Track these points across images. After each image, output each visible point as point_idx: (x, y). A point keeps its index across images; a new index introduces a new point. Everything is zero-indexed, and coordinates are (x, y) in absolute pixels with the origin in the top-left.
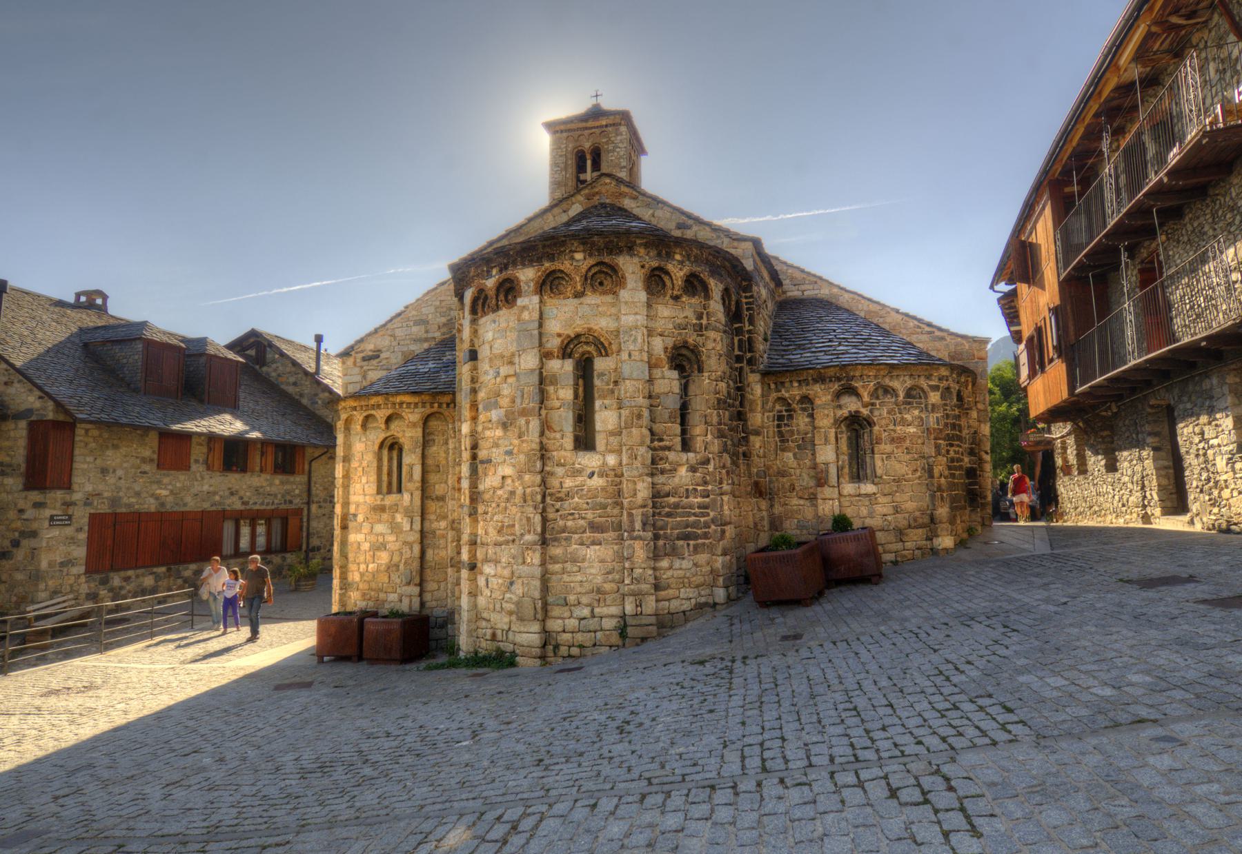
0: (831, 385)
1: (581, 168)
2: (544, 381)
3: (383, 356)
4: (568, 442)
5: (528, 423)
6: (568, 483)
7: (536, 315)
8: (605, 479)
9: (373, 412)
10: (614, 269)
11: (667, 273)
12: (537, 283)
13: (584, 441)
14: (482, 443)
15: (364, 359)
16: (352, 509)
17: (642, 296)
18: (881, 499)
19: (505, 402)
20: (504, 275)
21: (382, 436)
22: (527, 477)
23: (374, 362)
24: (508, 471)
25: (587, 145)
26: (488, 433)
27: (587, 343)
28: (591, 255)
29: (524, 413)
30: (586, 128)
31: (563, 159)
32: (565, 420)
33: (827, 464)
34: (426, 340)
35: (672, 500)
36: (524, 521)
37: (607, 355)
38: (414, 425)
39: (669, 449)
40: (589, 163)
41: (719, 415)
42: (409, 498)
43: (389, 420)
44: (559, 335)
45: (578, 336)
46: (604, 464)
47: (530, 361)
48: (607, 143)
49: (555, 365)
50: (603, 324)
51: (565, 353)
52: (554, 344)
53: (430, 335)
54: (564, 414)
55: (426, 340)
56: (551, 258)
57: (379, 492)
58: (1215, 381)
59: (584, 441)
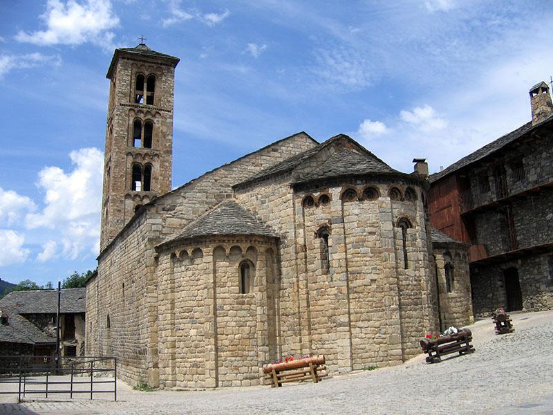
9: (239, 244)
10: (413, 191)
15: (163, 209)
16: (219, 302)
18: (458, 300)
20: (369, 185)
21: (241, 259)
24: (375, 277)
25: (147, 73)
29: (386, 250)
30: (147, 62)
37: (411, 227)
38: (262, 254)
40: (145, 85)
44: (397, 217)
46: (415, 275)
50: (409, 214)
52: (396, 220)
53: (208, 200)
56: (393, 182)
58: (542, 259)
59: (406, 267)
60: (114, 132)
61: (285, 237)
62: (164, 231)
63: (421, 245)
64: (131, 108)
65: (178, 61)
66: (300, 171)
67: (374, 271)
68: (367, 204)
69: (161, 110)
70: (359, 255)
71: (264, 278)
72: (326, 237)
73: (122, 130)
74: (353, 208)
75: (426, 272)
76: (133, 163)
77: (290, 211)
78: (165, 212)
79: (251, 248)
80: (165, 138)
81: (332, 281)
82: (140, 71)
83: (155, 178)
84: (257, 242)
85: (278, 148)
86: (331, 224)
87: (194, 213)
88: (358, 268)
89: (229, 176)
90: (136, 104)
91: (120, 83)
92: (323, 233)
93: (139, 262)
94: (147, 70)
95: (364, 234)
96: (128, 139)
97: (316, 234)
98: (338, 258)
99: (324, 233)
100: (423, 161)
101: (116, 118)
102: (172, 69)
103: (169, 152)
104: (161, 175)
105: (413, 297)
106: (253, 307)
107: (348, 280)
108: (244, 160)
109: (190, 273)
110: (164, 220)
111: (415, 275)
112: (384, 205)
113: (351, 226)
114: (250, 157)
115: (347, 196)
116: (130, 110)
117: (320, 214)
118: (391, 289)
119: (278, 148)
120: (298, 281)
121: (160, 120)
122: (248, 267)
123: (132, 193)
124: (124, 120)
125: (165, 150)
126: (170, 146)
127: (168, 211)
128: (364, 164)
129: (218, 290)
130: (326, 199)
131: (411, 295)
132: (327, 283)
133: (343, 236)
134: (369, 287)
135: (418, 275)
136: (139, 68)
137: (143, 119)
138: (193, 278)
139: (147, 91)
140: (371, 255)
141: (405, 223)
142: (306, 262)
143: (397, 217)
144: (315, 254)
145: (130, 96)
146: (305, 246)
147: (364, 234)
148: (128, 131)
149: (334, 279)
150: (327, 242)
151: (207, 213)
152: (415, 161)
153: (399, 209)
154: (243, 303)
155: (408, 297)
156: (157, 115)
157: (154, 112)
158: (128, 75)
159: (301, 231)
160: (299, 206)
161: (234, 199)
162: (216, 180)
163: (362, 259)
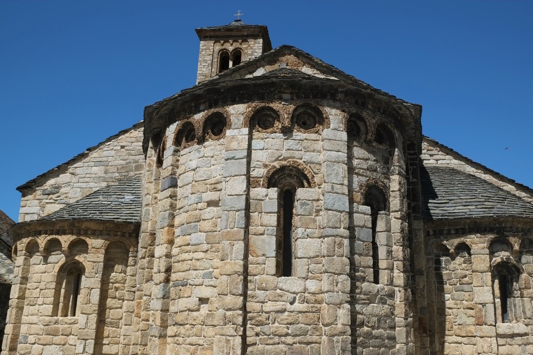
4: (271, 265)
6: (269, 306)
7: (245, 145)
8: (305, 304)
11: (362, 120)
13: (285, 267)
14: (176, 266)
17: (344, 136)
22: (229, 300)
23: (54, 197)
24: (205, 292)
25: (231, 48)
26: (185, 256)
27: (290, 176)
28: (298, 97)
29: (228, 236)
31: (210, 57)
32: (267, 245)
35: (366, 329)
36: (223, 343)
37: (310, 186)
39: (363, 279)
41: (403, 251)
42: (84, 320)
43: (73, 245)
44: (266, 166)
45: (283, 168)
46: (305, 290)
47: (239, 185)
49: (258, 192)
51: (271, 182)
57: (55, 313)
59: (285, 267)
67: (207, 281)
78: (46, 197)
82: (223, 47)
91: (201, 64)
95: (200, 205)
105: (289, 340)
106: (72, 339)
111: (305, 290)
112: (234, 145)
118: (226, 321)
127: (49, 194)
131: (287, 335)
134: (195, 314)
140: (205, 247)
143: (266, 166)
147: (200, 205)
154: (55, 334)
155: (276, 339)
158: (209, 55)
162: (123, 147)
163: (191, 255)
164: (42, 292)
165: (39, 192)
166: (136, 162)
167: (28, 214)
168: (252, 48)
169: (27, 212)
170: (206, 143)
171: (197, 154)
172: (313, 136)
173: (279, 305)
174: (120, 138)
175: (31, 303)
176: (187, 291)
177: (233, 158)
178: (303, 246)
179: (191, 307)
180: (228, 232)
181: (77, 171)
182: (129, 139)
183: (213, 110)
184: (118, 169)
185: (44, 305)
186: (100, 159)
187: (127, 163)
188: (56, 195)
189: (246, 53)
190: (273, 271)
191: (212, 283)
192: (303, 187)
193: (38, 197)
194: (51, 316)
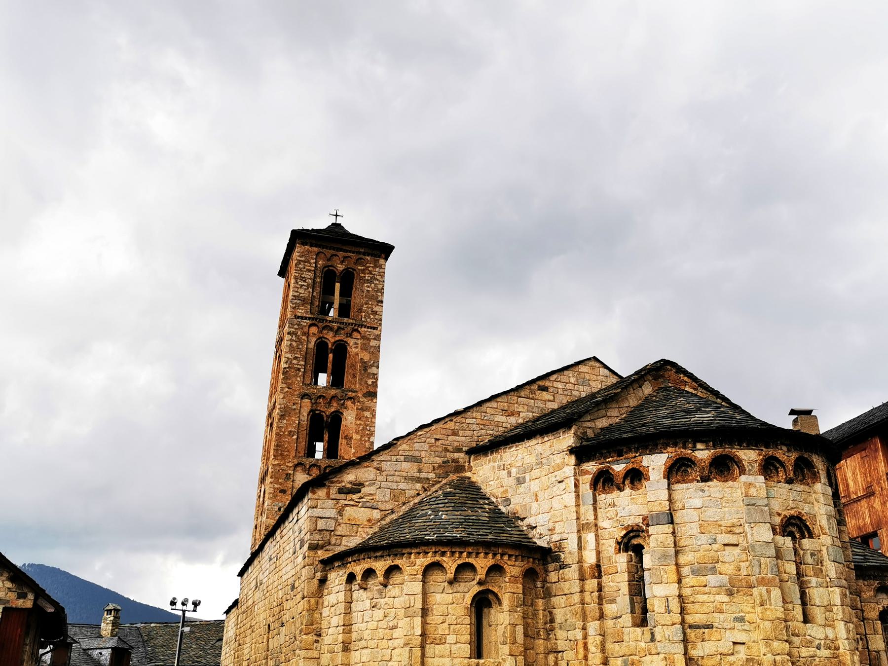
0: (872, 582)
1: (328, 290)
2: (779, 556)
3: (363, 490)
5: (768, 592)
9: (470, 560)
10: (810, 466)
12: (760, 465)
15: (341, 491)
19: (729, 569)
20: (719, 451)
21: (476, 589)
22: (776, 644)
23: (355, 497)
24: (741, 637)
25: (341, 267)
26: (701, 598)
29: (762, 582)
30: (341, 250)
31: (311, 275)
33: (878, 652)
34: (419, 480)
37: (811, 536)
38: (514, 579)
40: (338, 285)
44: (779, 515)
45: (792, 517)
46: (826, 638)
48: (363, 271)
49: (780, 539)
52: (777, 520)
53: (423, 475)
54: (792, 587)
55: (419, 480)
60: (283, 360)
61: (560, 548)
62: (340, 530)
63: (833, 574)
64: (314, 322)
65: (393, 248)
66: (588, 424)
67: (738, 625)
68: (715, 487)
69: (362, 326)
70: (707, 589)
71: (520, 629)
72: (638, 550)
73: (296, 358)
74: (692, 495)
75: (848, 631)
76: (311, 411)
77: (570, 499)
79: (496, 569)
80: (365, 370)
81: (653, 639)
82: (330, 263)
83: (346, 437)
84: (506, 558)
85: (547, 383)
86: (648, 525)
87: (395, 498)
88: (705, 616)
89: (461, 433)
90: (321, 317)
91: (297, 282)
92: (632, 542)
93: (293, 587)
94: (342, 262)
96: (304, 372)
97: (619, 543)
98: (663, 594)
99: (635, 542)
100: (808, 412)
101: (287, 337)
102: (382, 261)
103: (373, 395)
104: (357, 433)
107: (685, 641)
108: (488, 404)
109: (378, 614)
110: (340, 513)
111: (826, 638)
112: (752, 491)
113: (688, 528)
114: (499, 399)
115: (677, 470)
116: (311, 325)
117: (625, 507)
119: (547, 383)
120: (585, 637)
121: (359, 342)
122: (489, 605)
123: (308, 461)
124: (299, 341)
125: (365, 391)
126: (375, 384)
128: (708, 413)
129: (430, 649)
130: (636, 476)
132: (643, 644)
133: (672, 551)
134: (731, 659)
135: (831, 636)
136: (329, 260)
137: (333, 341)
138: (383, 624)
139: (341, 295)
141: (795, 526)
142: (600, 598)
143: (779, 515)
144: (618, 582)
145: (312, 304)
146: (598, 566)
148: (305, 359)
149: (658, 637)
150: (641, 561)
151: (417, 500)
152: (793, 412)
153: (785, 497)
156: (355, 334)
157: (349, 329)
159: (590, 537)
160: (586, 489)
161: (468, 474)
162: (437, 440)
164: (452, 627)
165: (333, 490)
166: (455, 461)
167: (321, 518)
168: (370, 273)
169: (320, 515)
170: (710, 483)
171: (701, 493)
172: (807, 488)
173: (812, 650)
174: (433, 428)
175: (438, 641)
176: (716, 635)
177: (753, 505)
178: (817, 594)
179: (725, 651)
180: (763, 578)
181: (384, 465)
182: (444, 432)
183: (719, 451)
184: (434, 469)
185: (458, 645)
186: (411, 453)
187: (444, 462)
188: (358, 495)
189: (361, 278)
190: (802, 619)
191: (745, 628)
192: (804, 537)
193: (332, 497)
194: (470, 658)
